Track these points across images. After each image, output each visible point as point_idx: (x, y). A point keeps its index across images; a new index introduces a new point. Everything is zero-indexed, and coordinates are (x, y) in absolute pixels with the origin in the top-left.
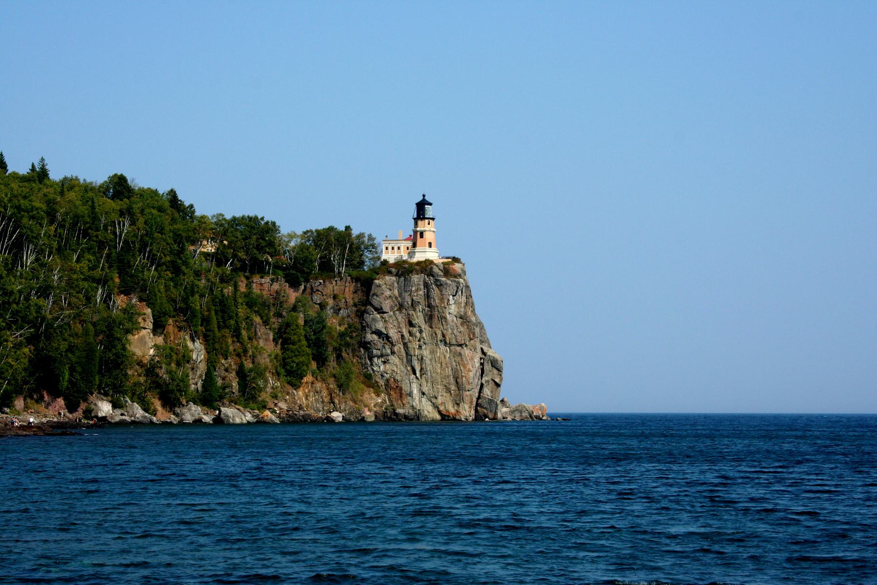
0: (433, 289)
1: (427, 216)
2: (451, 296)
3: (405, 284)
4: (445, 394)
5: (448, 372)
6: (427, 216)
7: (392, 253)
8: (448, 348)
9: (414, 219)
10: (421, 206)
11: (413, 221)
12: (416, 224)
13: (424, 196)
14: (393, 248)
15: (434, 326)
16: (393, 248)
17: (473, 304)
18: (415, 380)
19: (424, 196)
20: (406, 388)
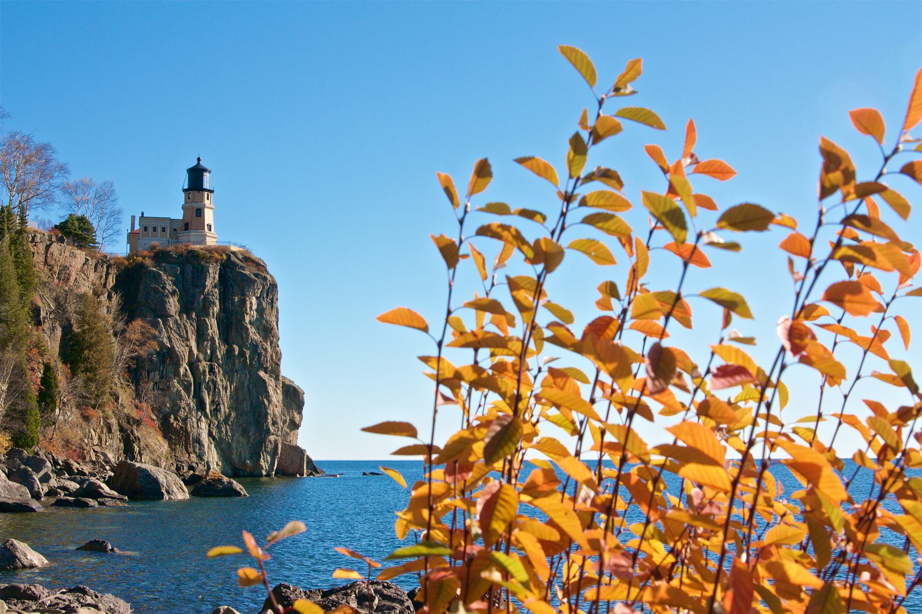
0: (231, 285)
1: (204, 187)
2: (254, 298)
3: (193, 277)
4: (241, 439)
5: (247, 407)
6: (204, 187)
7: (153, 236)
8: (247, 372)
9: (185, 190)
10: (196, 174)
11: (183, 194)
12: (187, 198)
13: (199, 160)
14: (155, 229)
15: (229, 339)
16: (155, 229)
17: (277, 309)
18: (203, 419)
19: (199, 160)
20: (194, 432)
